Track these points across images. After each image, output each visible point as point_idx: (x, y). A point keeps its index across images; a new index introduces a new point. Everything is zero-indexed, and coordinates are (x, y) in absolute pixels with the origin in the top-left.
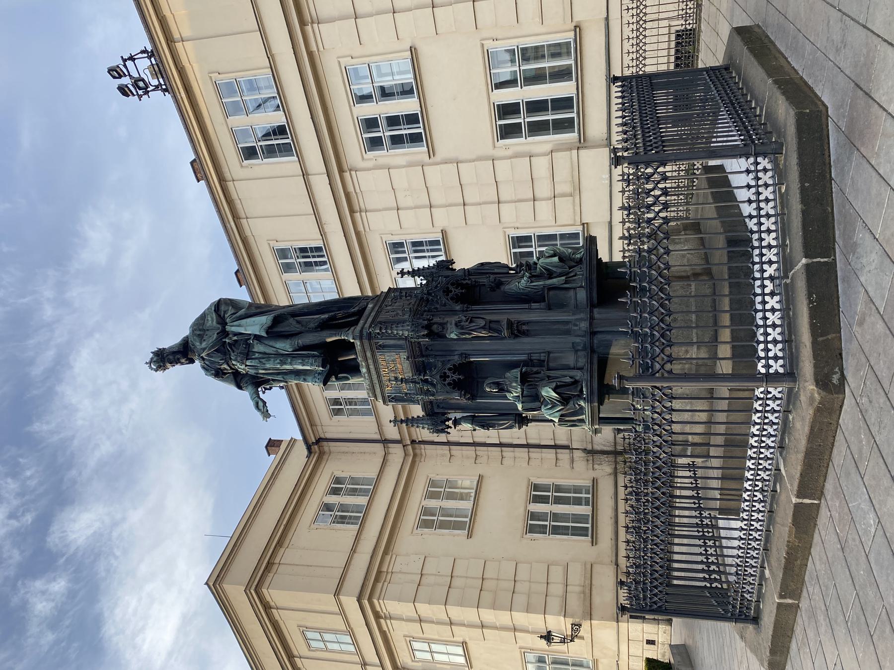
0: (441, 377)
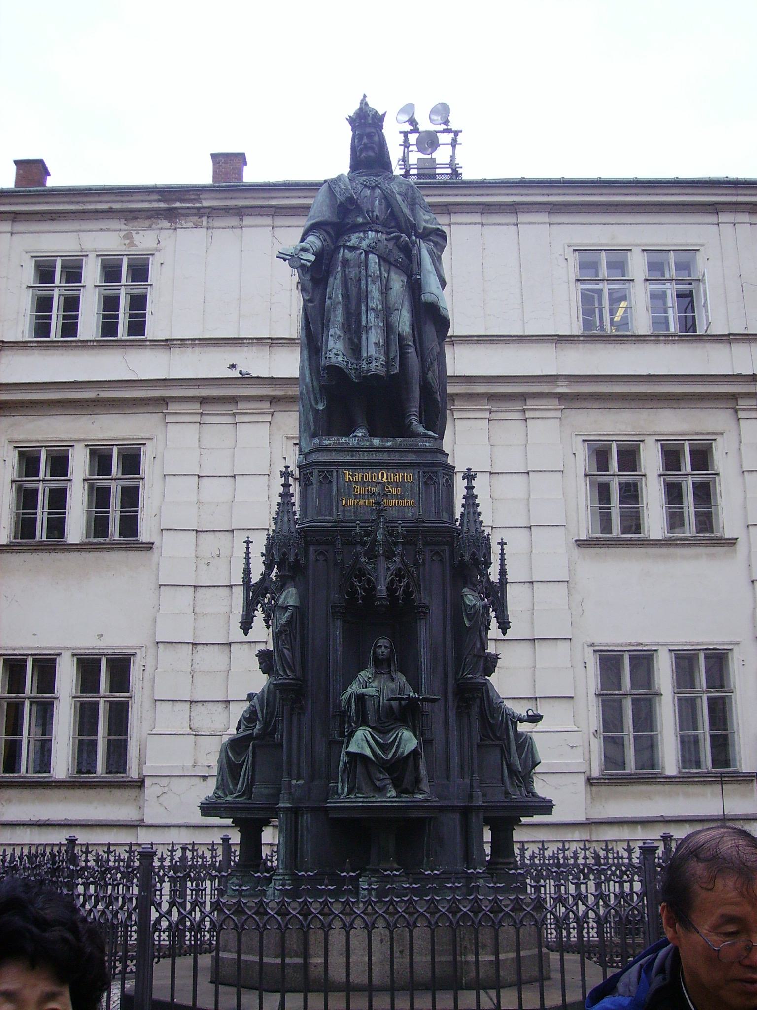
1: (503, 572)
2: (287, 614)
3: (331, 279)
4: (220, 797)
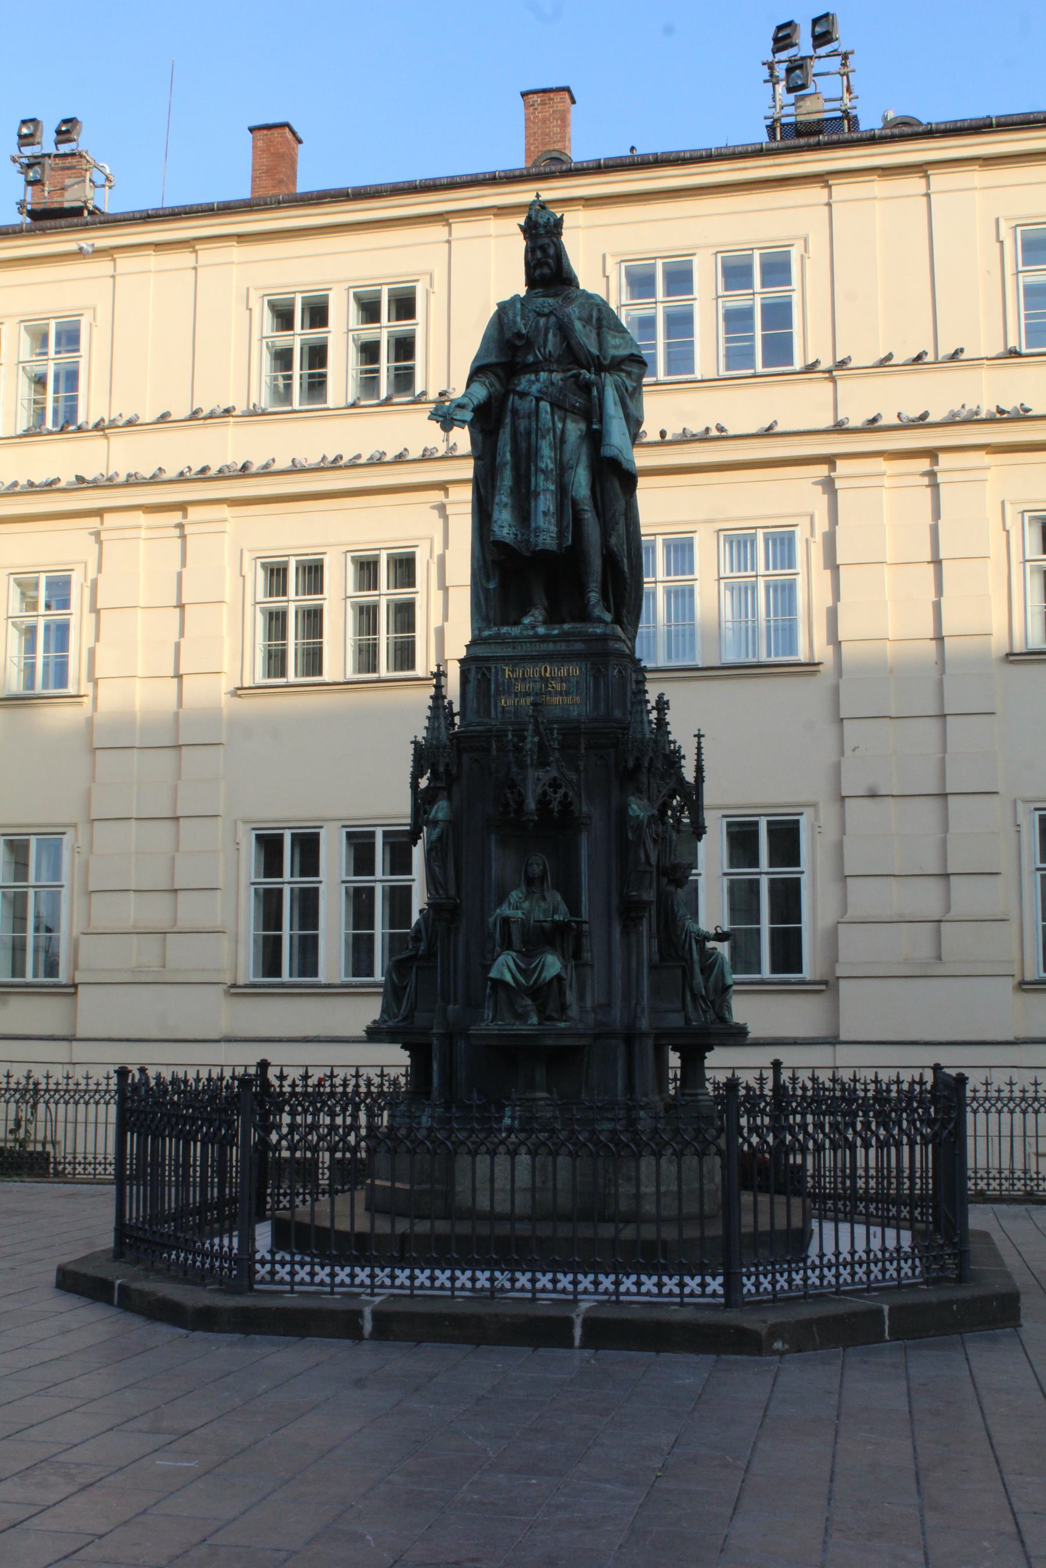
0: (555, 779)
1: (699, 769)
2: (438, 830)
3: (501, 431)
4: (385, 1021)
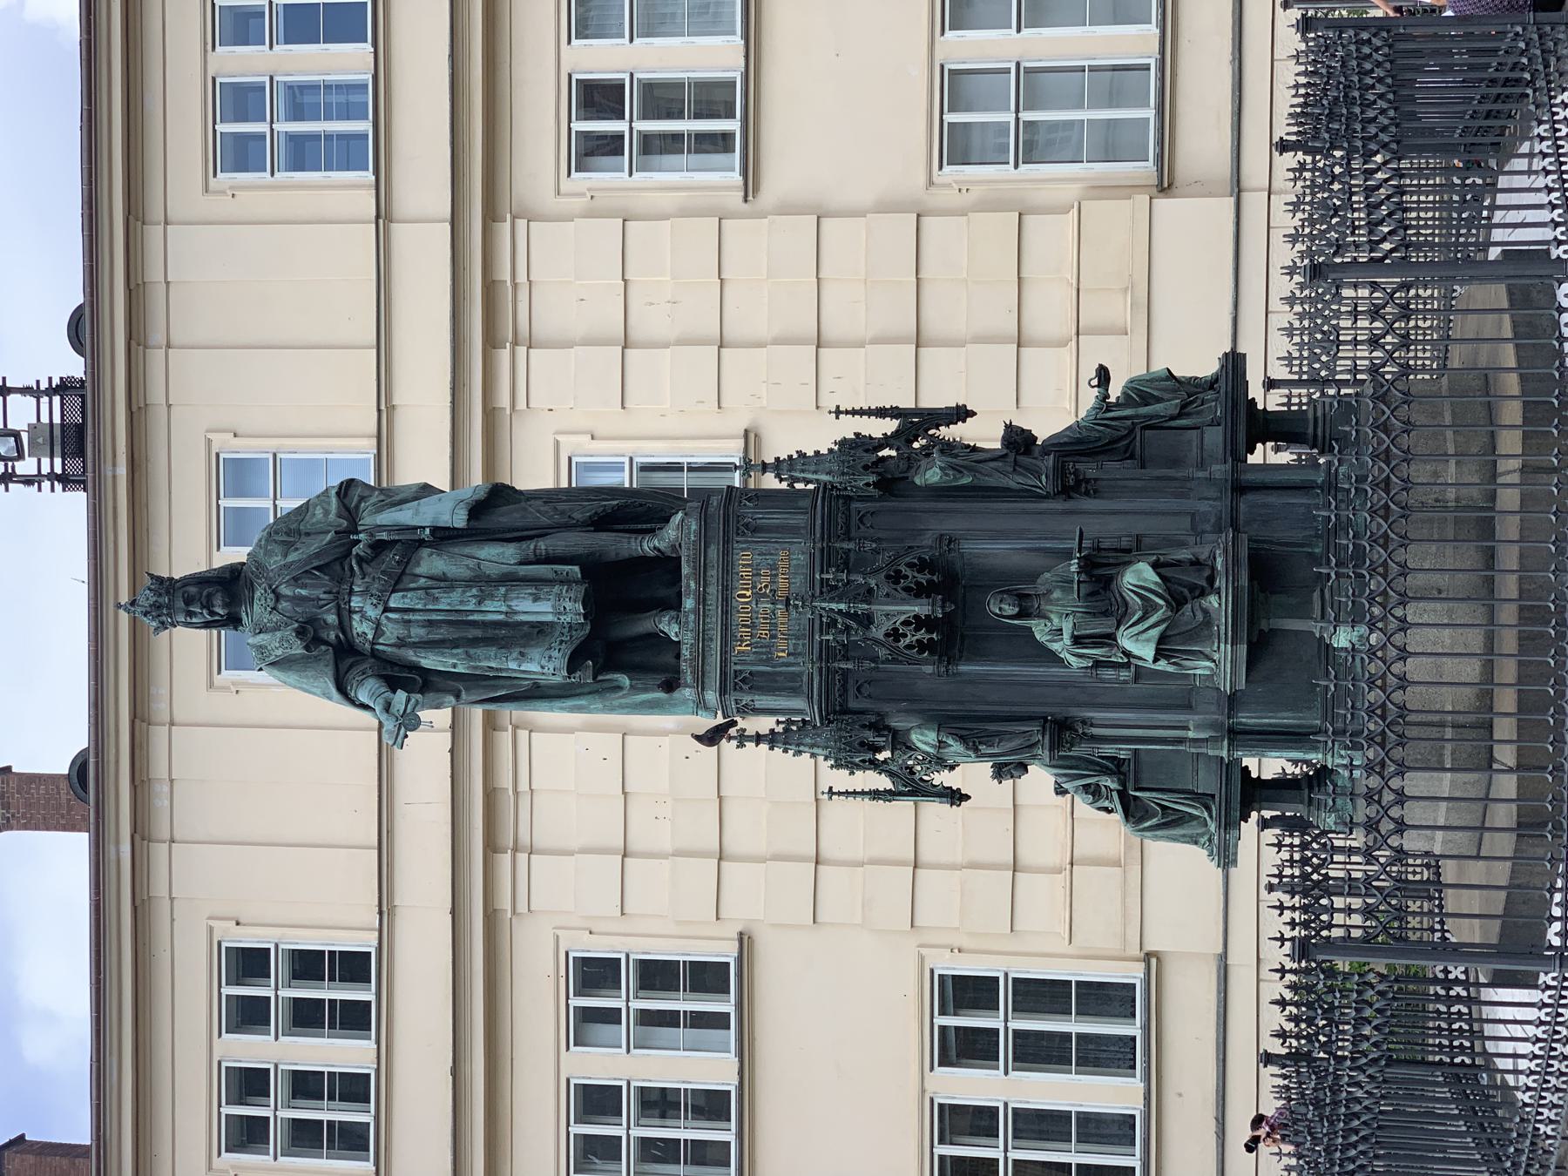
0: (888, 577)
1: (881, 413)
2: (950, 741)
